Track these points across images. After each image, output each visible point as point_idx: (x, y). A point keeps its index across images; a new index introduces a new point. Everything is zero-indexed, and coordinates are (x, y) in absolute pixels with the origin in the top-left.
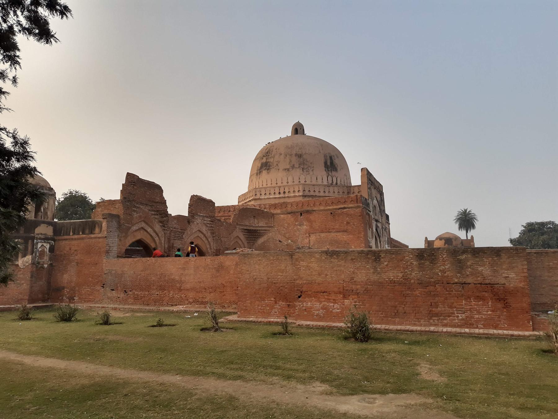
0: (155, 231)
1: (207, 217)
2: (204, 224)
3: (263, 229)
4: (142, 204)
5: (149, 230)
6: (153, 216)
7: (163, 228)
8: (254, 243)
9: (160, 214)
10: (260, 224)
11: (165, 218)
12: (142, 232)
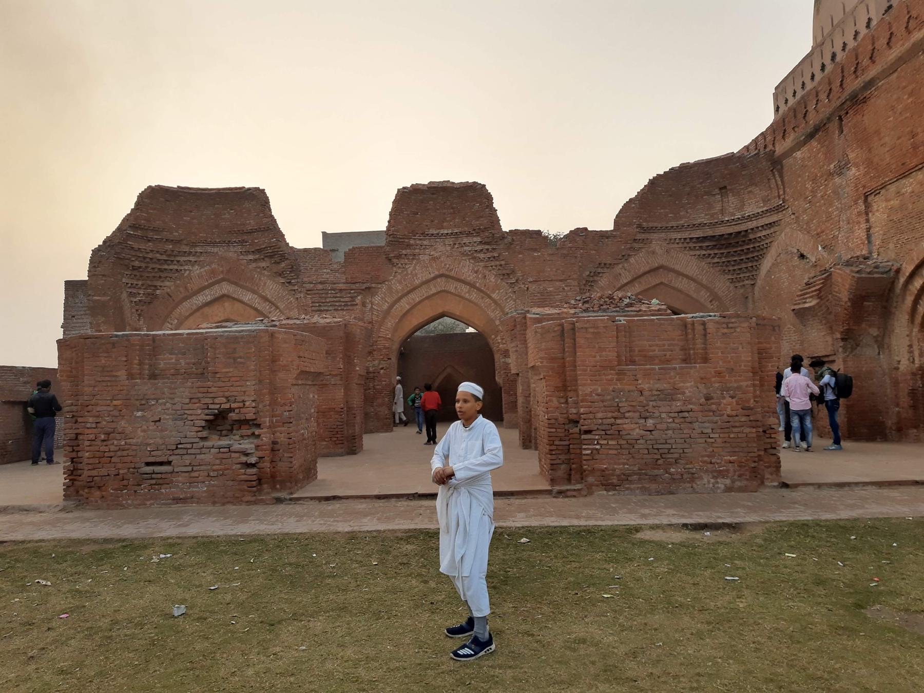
0: (265, 299)
1: (469, 234)
2: (463, 254)
3: (762, 222)
4: (213, 244)
5: (247, 297)
6: (254, 265)
7: (291, 287)
8: (754, 278)
9: (271, 257)
10: (744, 208)
11: (283, 265)
12: (226, 304)
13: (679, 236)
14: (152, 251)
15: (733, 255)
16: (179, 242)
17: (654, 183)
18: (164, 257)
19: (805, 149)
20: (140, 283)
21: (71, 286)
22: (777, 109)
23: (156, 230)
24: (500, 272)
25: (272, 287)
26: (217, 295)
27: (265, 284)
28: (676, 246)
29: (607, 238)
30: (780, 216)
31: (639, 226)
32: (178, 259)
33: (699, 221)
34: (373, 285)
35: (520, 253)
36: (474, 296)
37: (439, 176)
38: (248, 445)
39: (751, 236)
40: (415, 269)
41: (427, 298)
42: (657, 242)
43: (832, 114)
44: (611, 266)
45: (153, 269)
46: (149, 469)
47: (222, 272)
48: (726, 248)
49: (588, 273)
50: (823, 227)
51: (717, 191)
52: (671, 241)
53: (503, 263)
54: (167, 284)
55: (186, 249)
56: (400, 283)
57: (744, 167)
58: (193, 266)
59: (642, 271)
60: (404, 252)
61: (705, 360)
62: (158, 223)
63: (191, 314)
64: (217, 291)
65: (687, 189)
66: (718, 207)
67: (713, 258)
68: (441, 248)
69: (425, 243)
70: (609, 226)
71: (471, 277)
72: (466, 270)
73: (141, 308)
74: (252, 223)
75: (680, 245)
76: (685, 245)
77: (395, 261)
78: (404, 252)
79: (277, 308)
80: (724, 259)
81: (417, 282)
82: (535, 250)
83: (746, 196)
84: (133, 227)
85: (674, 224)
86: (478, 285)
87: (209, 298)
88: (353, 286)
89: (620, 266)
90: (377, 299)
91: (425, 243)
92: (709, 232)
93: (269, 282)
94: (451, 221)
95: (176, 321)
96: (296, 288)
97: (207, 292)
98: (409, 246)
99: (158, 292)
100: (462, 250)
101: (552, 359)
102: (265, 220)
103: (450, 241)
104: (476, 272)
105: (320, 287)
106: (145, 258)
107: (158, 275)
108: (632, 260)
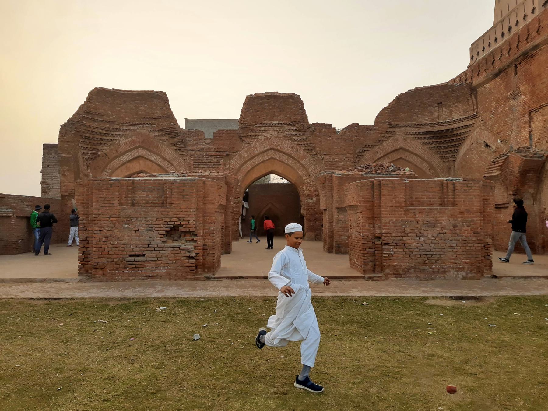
0: (165, 159)
1: (289, 125)
3: (462, 124)
4: (134, 124)
5: (154, 158)
6: (158, 138)
7: (181, 153)
8: (455, 157)
9: (169, 134)
10: (452, 115)
11: (177, 139)
12: (141, 162)
13: (412, 130)
14: (97, 128)
15: (443, 143)
16: (113, 123)
17: (399, 98)
18: (104, 132)
19: (492, 82)
20: (89, 147)
21: (47, 148)
22: (472, 58)
23: (100, 115)
24: (306, 148)
25: (169, 152)
26: (136, 156)
27: (165, 150)
28: (410, 136)
29: (371, 130)
30: (474, 121)
31: (390, 124)
32: (112, 133)
33: (425, 122)
34: (231, 153)
35: (319, 137)
36: (290, 162)
37: (271, 89)
38: (190, 246)
39: (455, 132)
40: (256, 144)
41: (262, 162)
42: (399, 134)
43: (511, 63)
44: (372, 147)
45: (97, 138)
46: (132, 259)
47: (139, 142)
48: (439, 139)
49: (358, 150)
50: (502, 129)
51: (436, 105)
52: (407, 133)
53: (308, 142)
54: (105, 148)
55: (118, 127)
56: (247, 152)
57: (454, 91)
58: (121, 137)
59: (390, 151)
60: (249, 134)
61: (454, 204)
62: (101, 111)
63: (119, 167)
64: (135, 153)
65: (419, 103)
66: (436, 114)
67: (432, 144)
68: (272, 133)
69: (262, 129)
70: (372, 123)
71: (289, 151)
72: (286, 146)
73: (89, 162)
74: (158, 113)
75: (413, 136)
76: (416, 136)
77: (244, 139)
78: (249, 134)
79: (172, 165)
80: (438, 145)
81: (257, 152)
82: (328, 136)
83: (454, 109)
84: (87, 113)
85: (409, 123)
86: (293, 155)
87: (130, 158)
88: (219, 154)
89: (377, 147)
90: (232, 162)
91: (262, 129)
92: (430, 129)
93: (167, 149)
94: (278, 116)
95: (110, 171)
96: (184, 153)
97: (129, 154)
98: (252, 130)
99: (99, 153)
100: (284, 134)
101: (367, 202)
102: (166, 112)
103: (277, 128)
104: (292, 148)
105: (199, 153)
106: (92, 132)
107: (99, 142)
108: (384, 144)
